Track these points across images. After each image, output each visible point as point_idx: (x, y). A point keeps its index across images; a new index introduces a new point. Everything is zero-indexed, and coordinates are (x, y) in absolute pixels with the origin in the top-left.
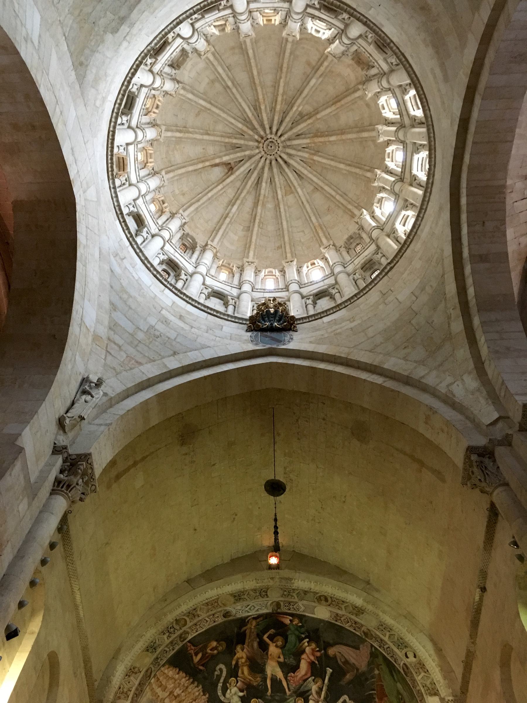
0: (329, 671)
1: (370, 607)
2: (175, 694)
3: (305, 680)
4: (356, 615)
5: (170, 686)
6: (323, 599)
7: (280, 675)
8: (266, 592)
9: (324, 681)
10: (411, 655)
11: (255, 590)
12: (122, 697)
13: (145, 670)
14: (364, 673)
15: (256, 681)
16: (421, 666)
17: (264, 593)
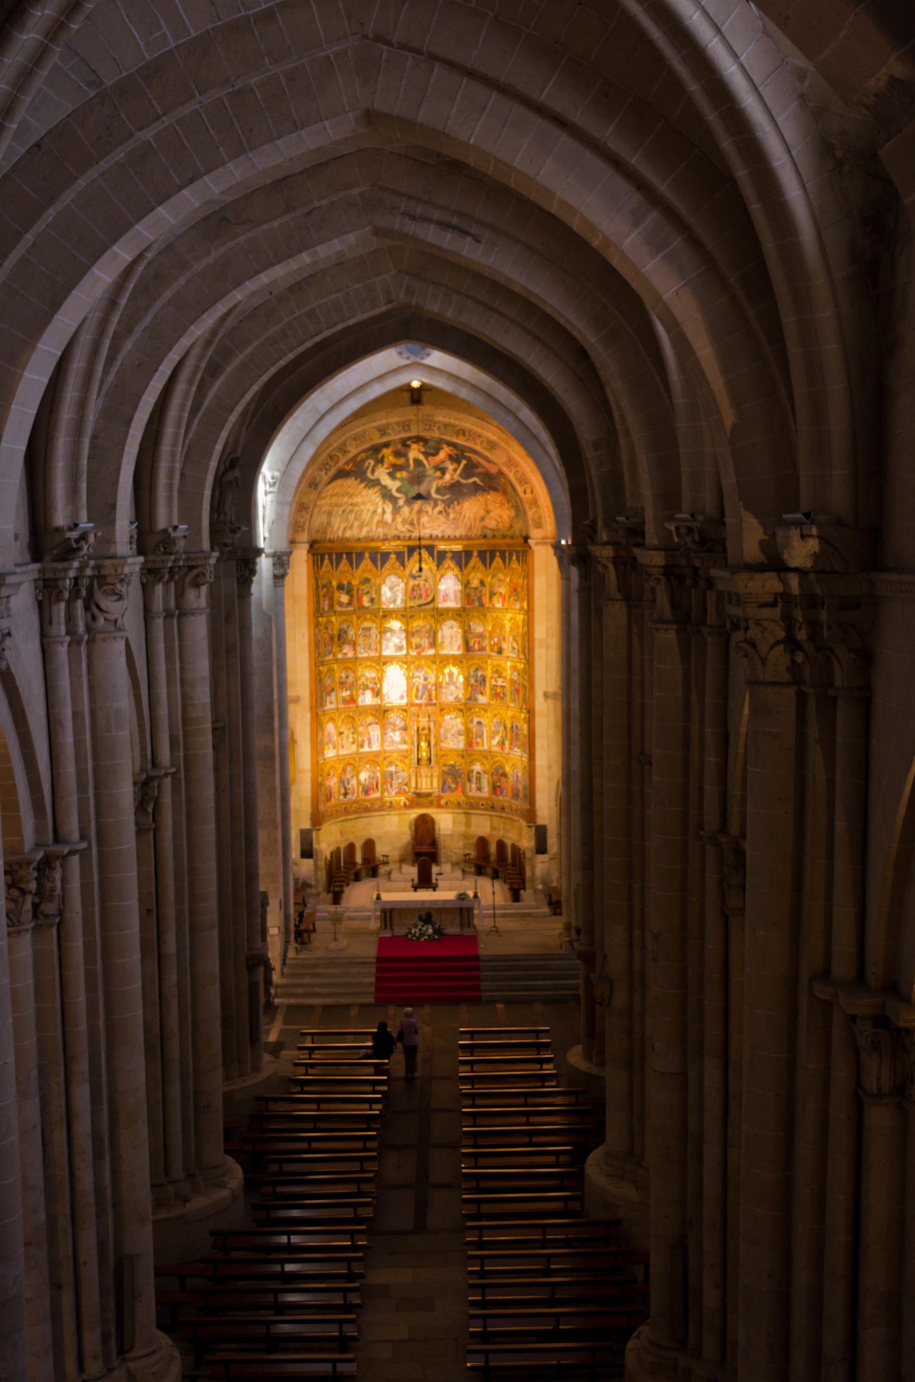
0: (464, 462)
1: (502, 444)
2: (334, 493)
3: (443, 462)
4: (490, 450)
5: (330, 493)
6: (462, 432)
7: (421, 457)
8: (409, 426)
9: (459, 465)
10: (528, 491)
11: (398, 424)
12: (300, 529)
13: (312, 506)
14: (492, 474)
15: (400, 462)
16: (535, 502)
17: (407, 428)
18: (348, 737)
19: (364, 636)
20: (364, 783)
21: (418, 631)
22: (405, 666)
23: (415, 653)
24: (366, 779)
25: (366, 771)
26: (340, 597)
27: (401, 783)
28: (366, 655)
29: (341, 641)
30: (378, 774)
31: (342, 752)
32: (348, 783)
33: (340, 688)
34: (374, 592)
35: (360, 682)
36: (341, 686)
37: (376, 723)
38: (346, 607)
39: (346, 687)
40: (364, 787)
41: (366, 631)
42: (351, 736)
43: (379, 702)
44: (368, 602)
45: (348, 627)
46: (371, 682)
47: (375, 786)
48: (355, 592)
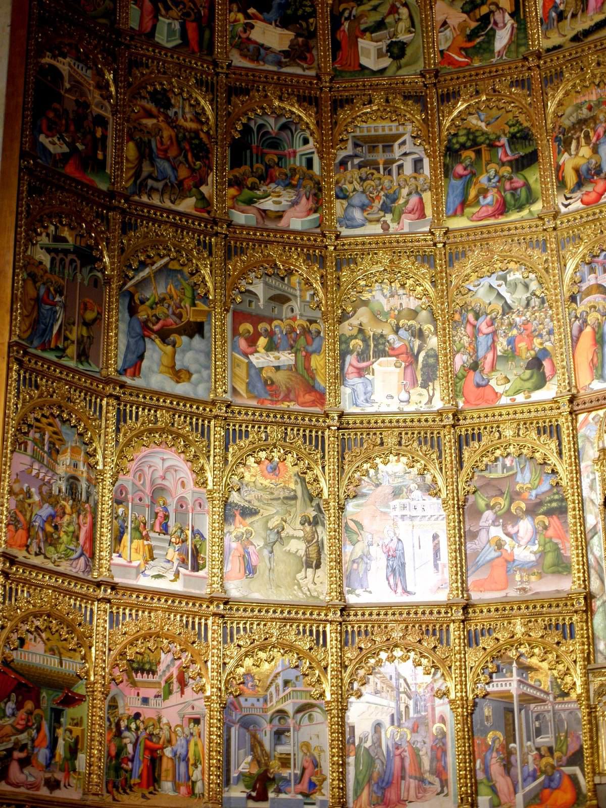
18: (279, 536)
19: (360, 167)
20: (368, 744)
21: (582, 122)
22: (536, 254)
23: (577, 205)
24: (378, 726)
25: (377, 692)
26: (252, 27)
27: (550, 750)
28: (377, 229)
29: (246, 168)
30: (442, 707)
31: (235, 590)
32: (279, 735)
33: (235, 332)
34: (402, 26)
35: (347, 328)
36: (247, 327)
37: (432, 491)
38: (280, 64)
39: (270, 334)
40: (371, 761)
41: (373, 149)
42: (295, 529)
43: (438, 404)
44: (380, 55)
45: (284, 127)
46: (396, 330)
47: (426, 764)
48: (322, 23)
